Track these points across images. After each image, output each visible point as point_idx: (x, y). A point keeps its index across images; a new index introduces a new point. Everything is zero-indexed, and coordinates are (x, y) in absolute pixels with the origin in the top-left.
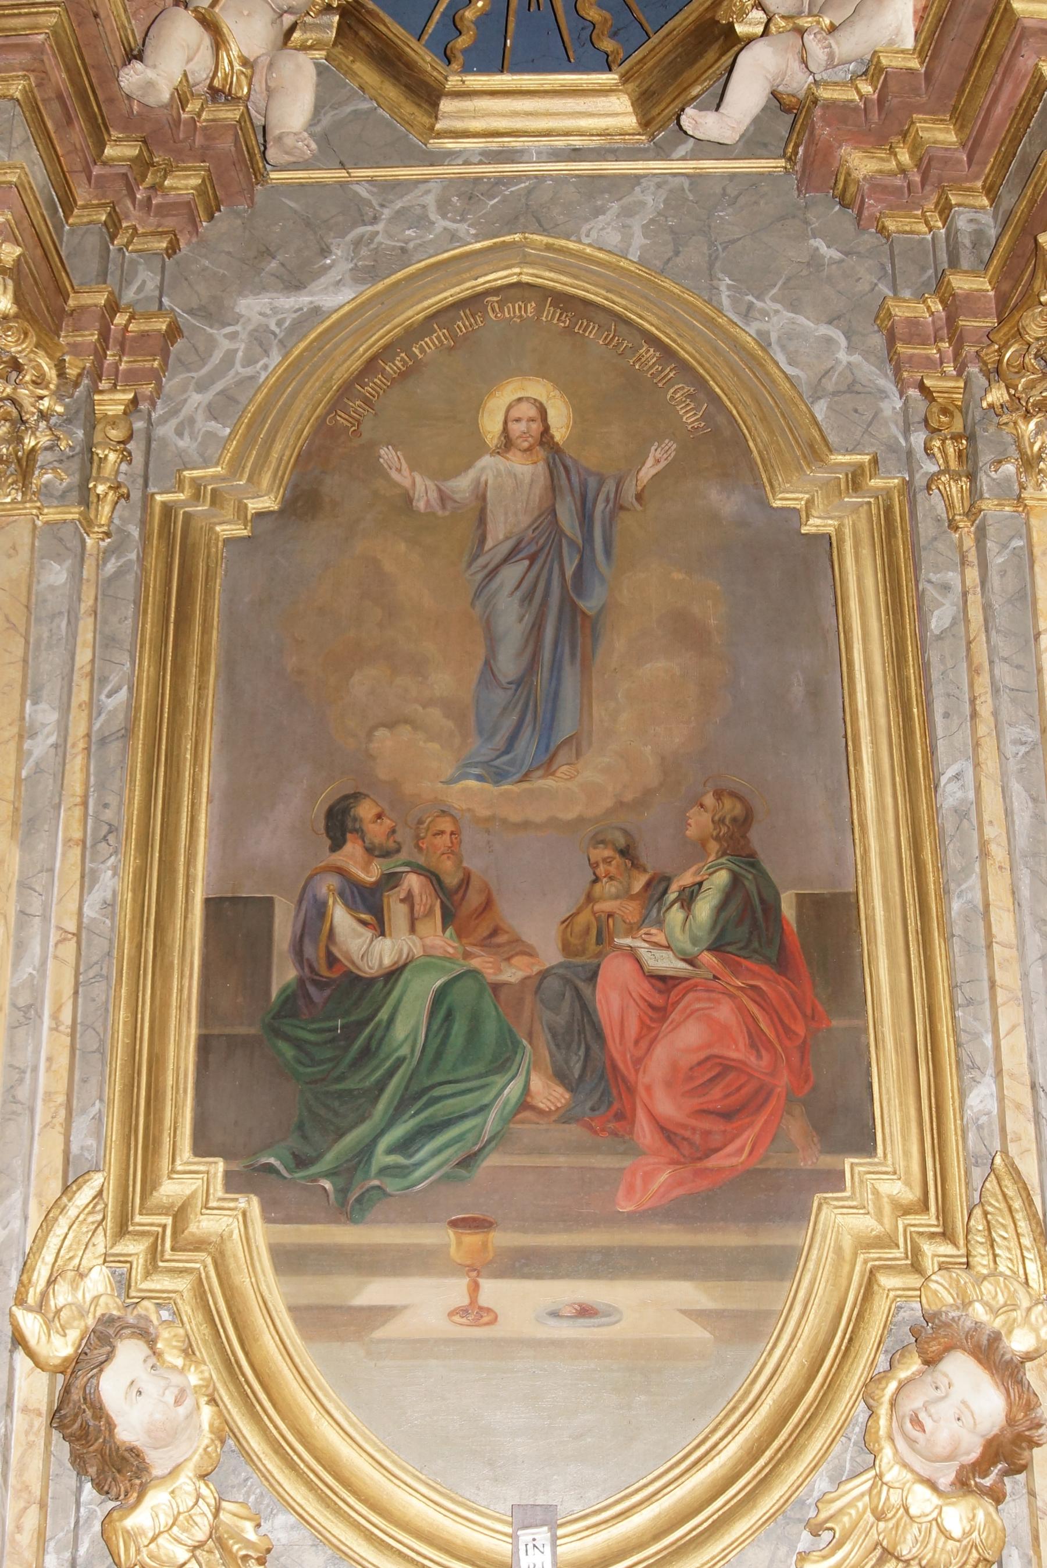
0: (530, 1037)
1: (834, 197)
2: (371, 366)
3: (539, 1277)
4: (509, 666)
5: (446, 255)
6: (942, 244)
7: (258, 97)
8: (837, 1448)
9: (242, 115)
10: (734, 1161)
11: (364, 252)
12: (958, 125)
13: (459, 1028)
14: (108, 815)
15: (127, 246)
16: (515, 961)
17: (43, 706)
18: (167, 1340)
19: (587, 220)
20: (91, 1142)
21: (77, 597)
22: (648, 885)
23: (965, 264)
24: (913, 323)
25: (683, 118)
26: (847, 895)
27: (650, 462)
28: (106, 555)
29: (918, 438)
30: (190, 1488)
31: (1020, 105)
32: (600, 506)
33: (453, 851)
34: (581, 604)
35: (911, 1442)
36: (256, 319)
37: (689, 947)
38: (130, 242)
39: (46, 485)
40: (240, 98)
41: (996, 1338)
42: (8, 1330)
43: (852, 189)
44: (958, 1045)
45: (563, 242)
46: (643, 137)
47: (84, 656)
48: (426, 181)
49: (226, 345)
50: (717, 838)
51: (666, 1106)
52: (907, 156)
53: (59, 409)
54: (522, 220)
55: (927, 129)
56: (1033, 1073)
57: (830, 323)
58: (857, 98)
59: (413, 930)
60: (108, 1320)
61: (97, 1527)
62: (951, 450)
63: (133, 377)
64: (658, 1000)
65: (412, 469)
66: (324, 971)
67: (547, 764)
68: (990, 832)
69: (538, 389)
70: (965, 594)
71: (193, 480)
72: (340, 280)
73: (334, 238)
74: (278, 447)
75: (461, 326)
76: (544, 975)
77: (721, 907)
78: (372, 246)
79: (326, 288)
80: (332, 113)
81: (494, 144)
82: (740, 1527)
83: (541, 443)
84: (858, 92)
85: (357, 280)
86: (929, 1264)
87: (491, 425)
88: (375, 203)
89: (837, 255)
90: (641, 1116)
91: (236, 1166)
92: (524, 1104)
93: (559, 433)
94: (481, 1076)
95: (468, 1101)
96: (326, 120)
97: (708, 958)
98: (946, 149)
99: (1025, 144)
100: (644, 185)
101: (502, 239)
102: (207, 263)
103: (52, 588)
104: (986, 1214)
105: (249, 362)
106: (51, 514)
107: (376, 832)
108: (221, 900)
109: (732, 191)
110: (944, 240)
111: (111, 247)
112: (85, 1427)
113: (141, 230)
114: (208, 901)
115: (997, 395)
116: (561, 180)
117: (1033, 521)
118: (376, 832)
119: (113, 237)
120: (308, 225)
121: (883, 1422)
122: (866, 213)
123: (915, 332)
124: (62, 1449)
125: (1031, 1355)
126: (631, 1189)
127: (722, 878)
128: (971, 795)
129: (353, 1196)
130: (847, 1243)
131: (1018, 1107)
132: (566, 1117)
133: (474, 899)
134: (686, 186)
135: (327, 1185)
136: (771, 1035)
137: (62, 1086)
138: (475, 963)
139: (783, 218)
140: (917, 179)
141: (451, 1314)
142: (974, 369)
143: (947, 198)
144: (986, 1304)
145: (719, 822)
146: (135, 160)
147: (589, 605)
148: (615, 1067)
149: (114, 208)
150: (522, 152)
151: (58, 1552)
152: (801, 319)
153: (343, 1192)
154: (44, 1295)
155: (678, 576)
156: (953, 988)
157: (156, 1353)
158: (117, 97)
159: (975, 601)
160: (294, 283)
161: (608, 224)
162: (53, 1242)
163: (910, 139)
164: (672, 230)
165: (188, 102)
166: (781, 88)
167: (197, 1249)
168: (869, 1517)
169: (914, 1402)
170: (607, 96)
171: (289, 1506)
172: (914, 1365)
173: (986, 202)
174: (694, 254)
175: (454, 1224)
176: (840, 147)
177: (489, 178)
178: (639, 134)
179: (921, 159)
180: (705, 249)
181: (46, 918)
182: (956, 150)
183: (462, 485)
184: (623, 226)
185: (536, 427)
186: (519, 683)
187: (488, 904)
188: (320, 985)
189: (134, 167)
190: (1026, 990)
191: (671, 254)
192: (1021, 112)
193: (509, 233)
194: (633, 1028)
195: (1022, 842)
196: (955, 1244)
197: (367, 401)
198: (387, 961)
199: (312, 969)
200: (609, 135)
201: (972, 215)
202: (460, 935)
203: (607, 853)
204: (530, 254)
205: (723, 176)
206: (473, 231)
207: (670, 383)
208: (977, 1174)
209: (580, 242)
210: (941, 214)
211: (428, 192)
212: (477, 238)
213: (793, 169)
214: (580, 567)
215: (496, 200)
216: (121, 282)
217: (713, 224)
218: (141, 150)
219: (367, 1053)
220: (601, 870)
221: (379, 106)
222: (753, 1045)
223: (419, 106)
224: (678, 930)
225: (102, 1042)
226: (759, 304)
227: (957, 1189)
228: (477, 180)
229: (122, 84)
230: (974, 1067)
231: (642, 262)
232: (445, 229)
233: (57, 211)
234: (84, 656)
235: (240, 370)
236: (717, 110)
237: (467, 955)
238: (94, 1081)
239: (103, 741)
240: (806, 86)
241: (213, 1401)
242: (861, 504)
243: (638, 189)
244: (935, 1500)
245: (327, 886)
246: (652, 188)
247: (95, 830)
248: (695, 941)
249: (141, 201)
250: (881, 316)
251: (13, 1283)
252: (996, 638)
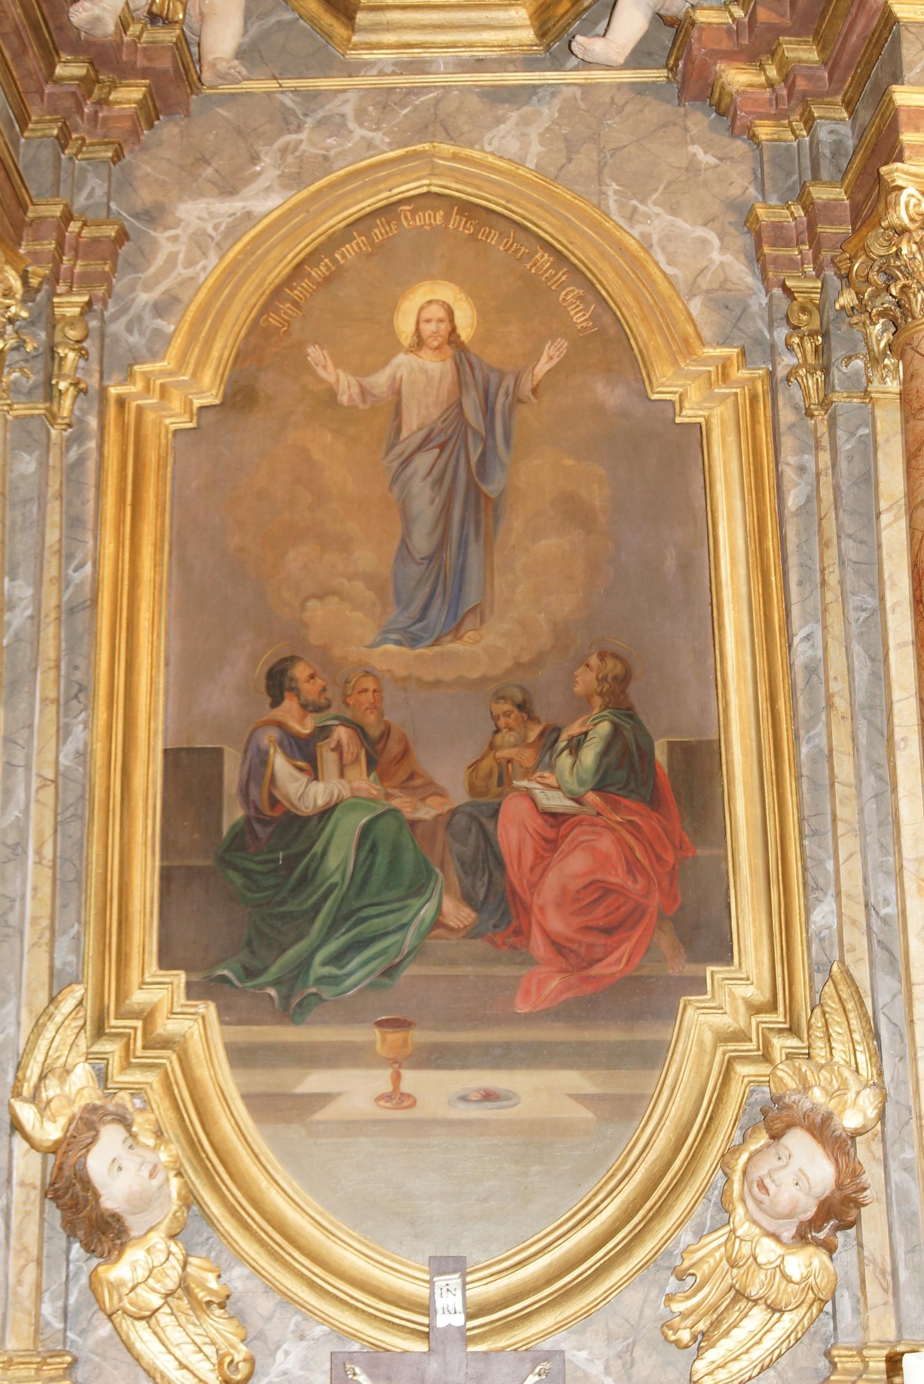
0: (442, 866)
1: (711, 105)
2: (298, 271)
3: (451, 1067)
4: (422, 543)
5: (364, 163)
6: (806, 151)
7: (194, 21)
8: (699, 1208)
9: (178, 37)
10: (614, 969)
11: (290, 159)
12: (820, 47)
13: (382, 859)
14: (78, 675)
15: (76, 155)
16: (430, 801)
17: (20, 582)
18: (141, 1123)
19: (489, 128)
20: (72, 958)
21: (44, 483)
22: (541, 735)
23: (825, 175)
24: (778, 227)
25: (574, 44)
26: (710, 742)
27: (544, 358)
28: (69, 443)
29: (781, 333)
30: (161, 1246)
31: (873, 34)
32: (501, 399)
33: (375, 706)
34: (485, 488)
35: (759, 1203)
36: (195, 224)
37: (575, 788)
38: (79, 151)
39: (15, 383)
40: (176, 22)
41: (828, 1118)
42: (7, 1118)
43: (726, 100)
44: (805, 869)
45: (466, 152)
46: (540, 48)
47: (52, 536)
48: (345, 91)
49: (167, 248)
50: (601, 694)
51: (557, 924)
52: (775, 72)
53: (24, 314)
54: (431, 128)
55: (793, 50)
56: (866, 894)
57: (705, 224)
58: (730, 20)
59: (342, 775)
60: (92, 1109)
61: (84, 1280)
62: (808, 346)
63: (87, 281)
64: (550, 833)
65: (336, 365)
66: (269, 812)
67: (455, 630)
68: (834, 687)
69: (447, 292)
70: (818, 475)
71: (144, 373)
72: (269, 187)
73: (263, 146)
74: (218, 345)
75: (378, 233)
76: (454, 812)
77: (604, 754)
78: (297, 154)
79: (256, 194)
80: (258, 24)
81: (406, 55)
82: (619, 1274)
83: (449, 343)
84: (731, 15)
85: (286, 187)
86: (778, 1055)
87: (405, 326)
88: (299, 112)
89: (712, 160)
90: (536, 933)
91: (196, 978)
92: (437, 923)
93: (465, 333)
94: (400, 899)
95: (390, 921)
96: (253, 31)
97: (592, 797)
98: (810, 68)
99: (877, 70)
100: (540, 95)
101: (413, 148)
102: (149, 170)
103: (23, 477)
104: (824, 1013)
105: (190, 263)
106: (20, 410)
107: (310, 690)
108: (179, 750)
109: (620, 99)
110: (808, 147)
111: (63, 156)
112: (75, 1197)
113: (88, 141)
114: (166, 751)
115: (848, 299)
116: (465, 90)
117: (878, 412)
118: (310, 690)
119: (63, 147)
120: (239, 132)
121: (736, 1186)
122: (738, 123)
123: (779, 235)
124: (55, 1215)
125: (859, 1131)
126: (527, 993)
127: (605, 728)
128: (820, 653)
129: (295, 1001)
130: (708, 1037)
131: (854, 922)
132: (472, 933)
133: (394, 748)
134: (579, 95)
135: (273, 992)
136: (645, 862)
137: (46, 911)
138: (395, 803)
139: (665, 125)
140: (785, 92)
141: (378, 1099)
142: (830, 272)
143: (810, 110)
144: (824, 1089)
145: (602, 680)
146: (81, 79)
147: (491, 489)
148: (514, 892)
149: (64, 123)
150: (430, 62)
151: (53, 1300)
152: (679, 222)
153: (286, 998)
154: (37, 1088)
155: (568, 462)
156: (801, 820)
157: (133, 1136)
158: (65, 26)
159: (826, 481)
160: (229, 190)
161: (508, 132)
162: (43, 1044)
163: (777, 58)
164: (566, 139)
165: (129, 26)
166: (662, 12)
167: (163, 1048)
168: (725, 1265)
169: (761, 1170)
170: (506, 10)
171: (242, 1259)
172: (763, 1139)
173: (845, 115)
174: (586, 160)
175: (380, 1024)
176: (715, 64)
177: (401, 88)
178: (536, 45)
179: (787, 75)
180: (595, 156)
181: (28, 768)
182: (818, 68)
183: (380, 381)
184: (522, 135)
185: (444, 327)
186: (430, 558)
187: (406, 753)
188: (265, 822)
189: (82, 85)
190: (861, 822)
191: (564, 161)
192: (874, 40)
193: (420, 142)
194: (529, 857)
195: (860, 697)
196: (800, 1038)
197: (295, 304)
198: (320, 802)
199: (257, 809)
200: (509, 46)
201: (833, 126)
202: (382, 778)
203: (507, 707)
204: (439, 165)
205: (611, 85)
206: (387, 140)
207: (562, 286)
208: (819, 978)
209: (483, 150)
210: (805, 123)
211: (347, 101)
212: (393, 146)
213: (674, 78)
214: (483, 454)
215: (408, 110)
216: (72, 188)
217: (602, 133)
218: (88, 70)
219: (305, 880)
220: (502, 722)
221: (301, 17)
222: (630, 871)
223: (337, 18)
224: (567, 773)
225: (79, 873)
226: (642, 208)
227: (802, 990)
228: (390, 90)
229: (72, 19)
230: (817, 888)
231: (539, 169)
232: (363, 137)
233: (14, 127)
234: (52, 536)
235: (182, 271)
236: (604, 36)
237: (388, 796)
238: (73, 907)
239: (72, 611)
240: (684, 10)
241: (179, 1174)
242: (728, 396)
243: (535, 99)
244: (779, 1250)
245: (268, 738)
246: (548, 98)
247: (67, 689)
248: (581, 783)
249: (88, 115)
250: (749, 221)
251: (10, 1078)
252: (844, 518)
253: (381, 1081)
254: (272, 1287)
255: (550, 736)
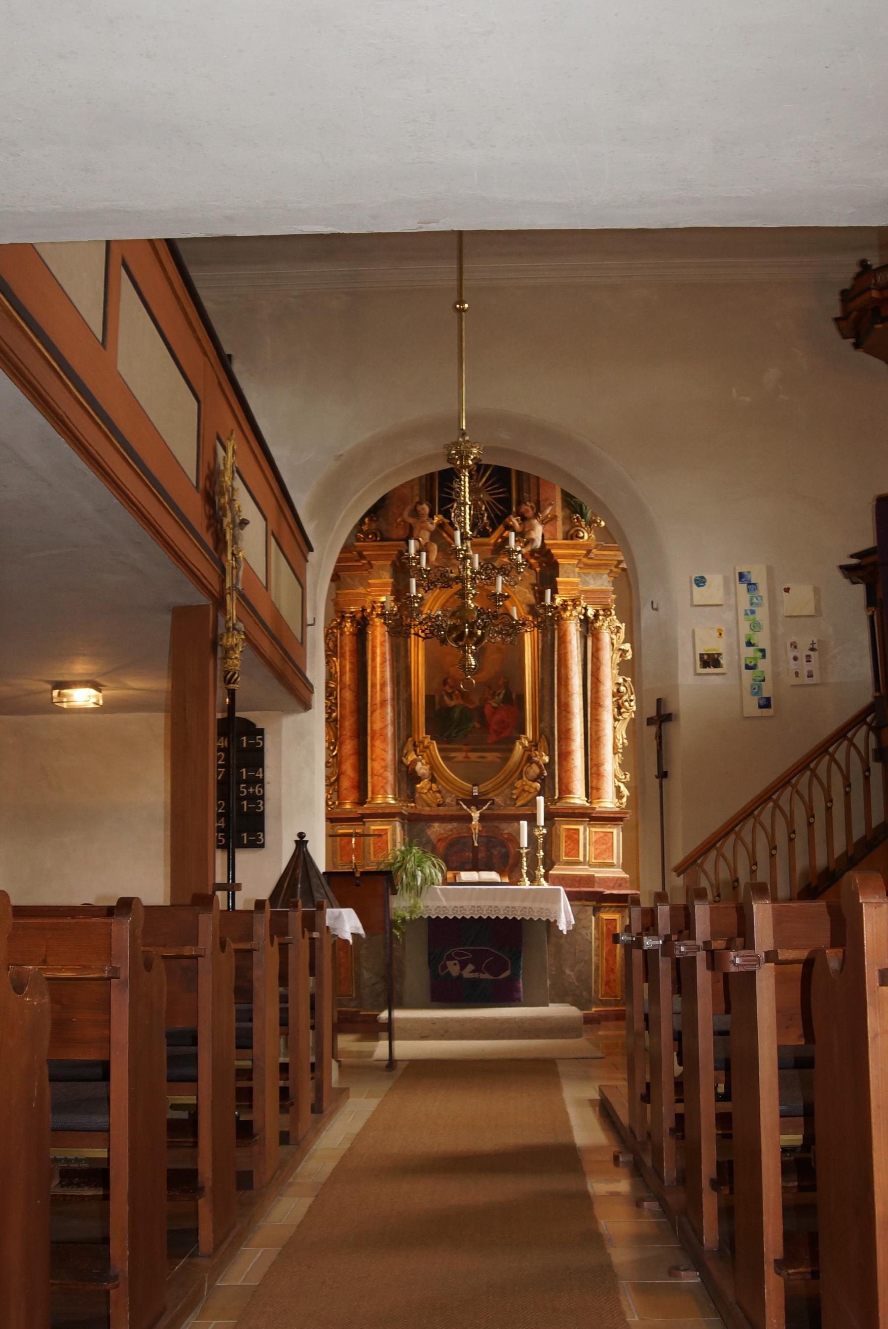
77: (504, 696)
97: (502, 705)
127: (504, 691)
245: (444, 693)
253: (464, 754)
254: (445, 788)
255: (495, 692)
